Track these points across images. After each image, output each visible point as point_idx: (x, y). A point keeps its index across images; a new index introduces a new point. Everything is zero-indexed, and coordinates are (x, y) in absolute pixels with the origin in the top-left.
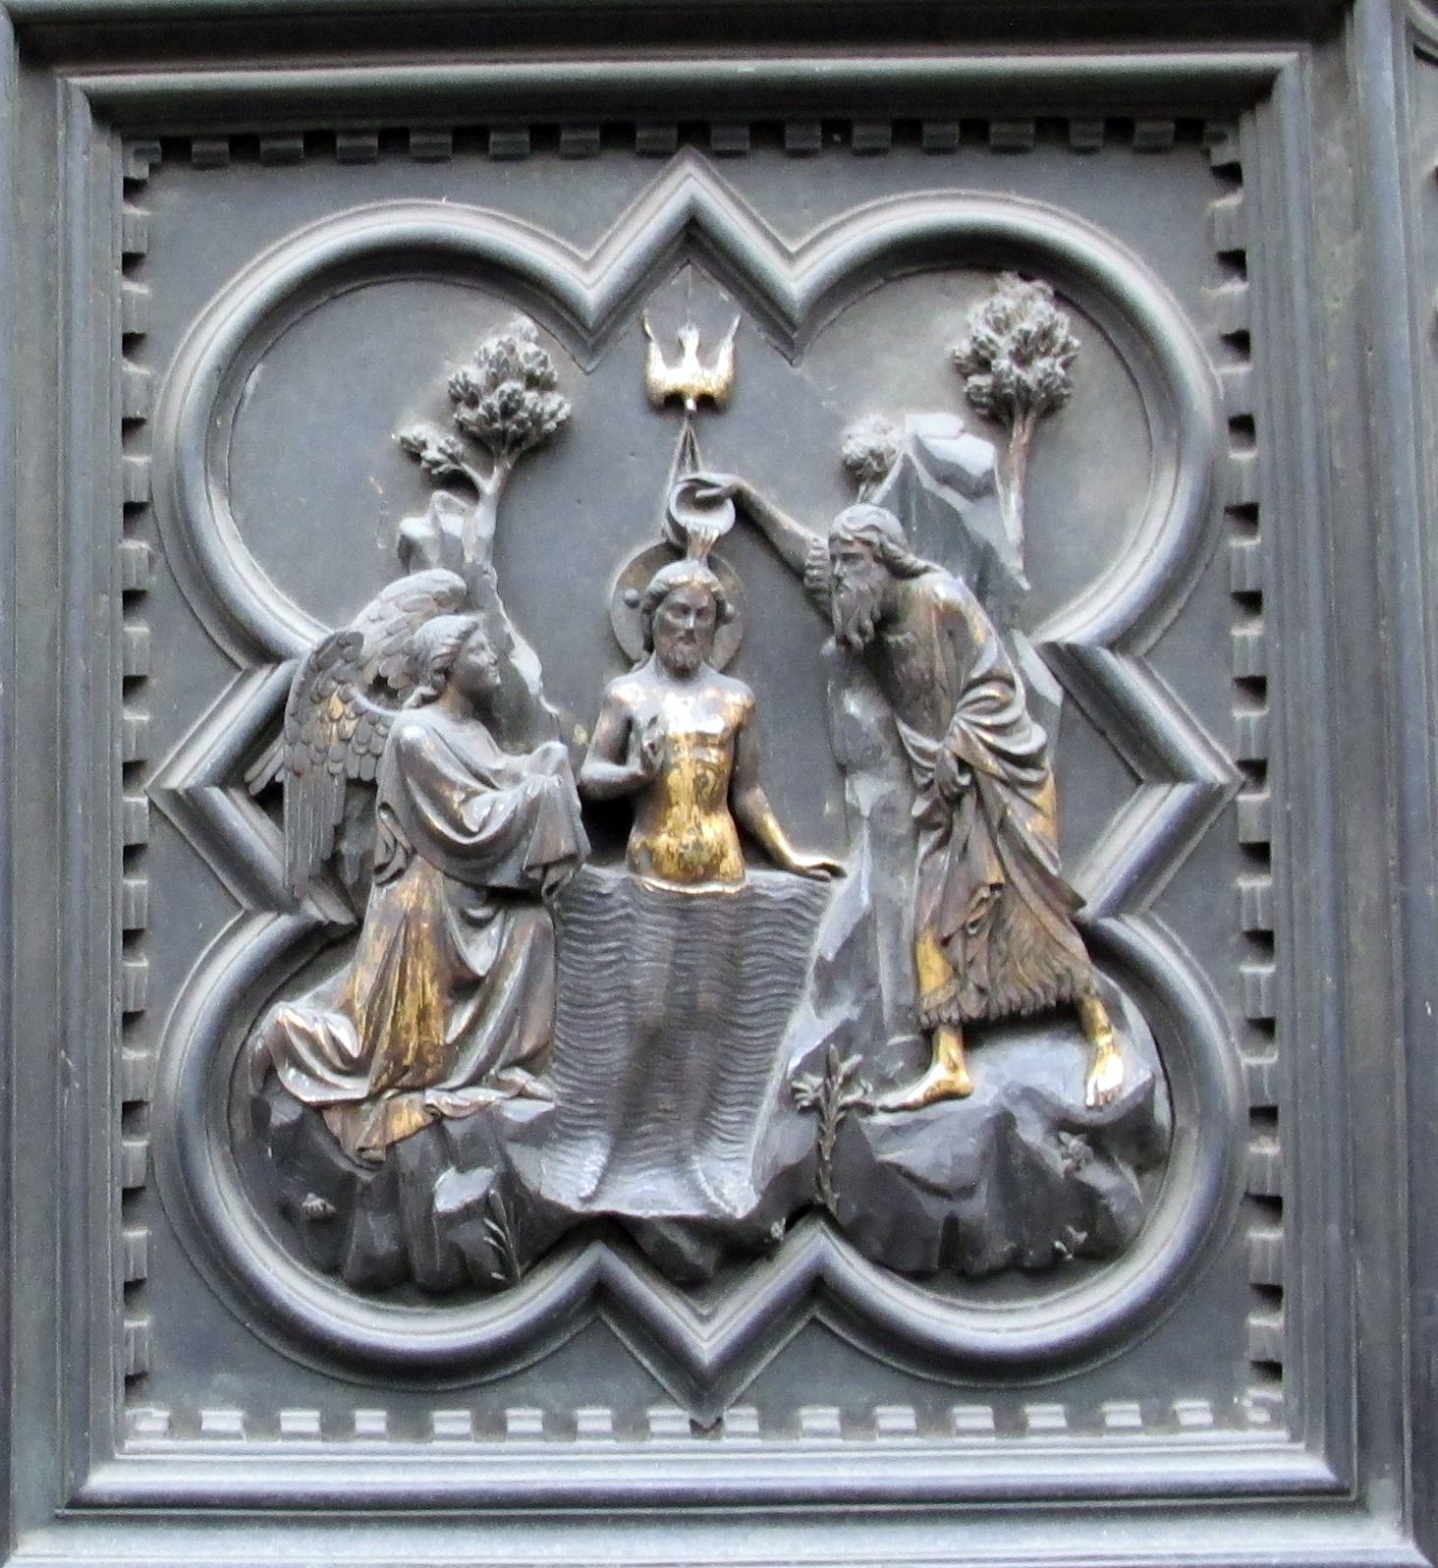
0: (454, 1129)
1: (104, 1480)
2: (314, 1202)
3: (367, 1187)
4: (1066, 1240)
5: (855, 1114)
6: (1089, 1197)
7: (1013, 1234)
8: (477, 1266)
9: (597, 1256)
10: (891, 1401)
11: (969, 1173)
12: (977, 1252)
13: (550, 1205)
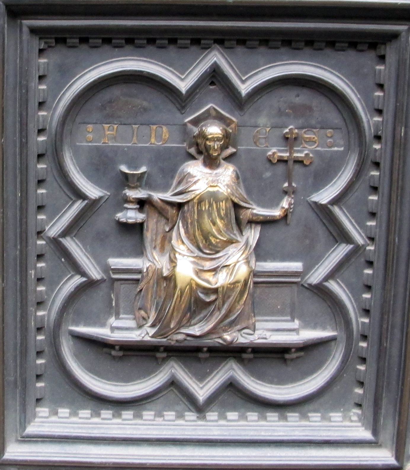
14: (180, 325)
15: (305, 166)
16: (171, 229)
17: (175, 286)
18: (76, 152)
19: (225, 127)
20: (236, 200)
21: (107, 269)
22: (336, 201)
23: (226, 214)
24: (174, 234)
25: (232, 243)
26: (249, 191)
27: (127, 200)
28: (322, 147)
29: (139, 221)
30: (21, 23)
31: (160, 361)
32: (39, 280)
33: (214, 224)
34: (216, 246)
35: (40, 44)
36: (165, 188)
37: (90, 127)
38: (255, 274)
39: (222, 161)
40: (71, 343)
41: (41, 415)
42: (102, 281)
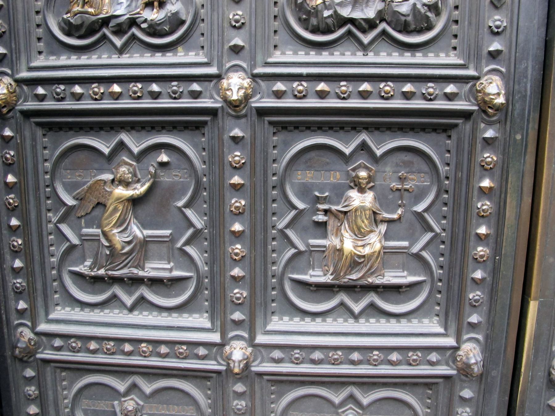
0: (327, 3)
1: (270, 60)
2: (304, 16)
3: (313, 12)
4: (423, 25)
5: (391, 3)
6: (428, 17)
7: (415, 25)
8: (330, 26)
9: (349, 26)
10: (395, 52)
11: (409, 12)
12: (409, 26)
13: (342, 16)
14: (345, 274)
15: (410, 192)
16: (341, 225)
17: (343, 254)
18: (292, 185)
19: (369, 172)
20: (374, 210)
21: (308, 245)
22: (426, 210)
23: (369, 217)
24: (343, 227)
25: (372, 232)
26: (381, 205)
27: (318, 210)
28: (419, 183)
29: (325, 220)
30: (264, 119)
31: (335, 292)
32: (273, 251)
33: (363, 222)
34: (364, 234)
35: (273, 130)
36: (338, 204)
37: (299, 172)
38: (384, 248)
39: (367, 190)
40: (290, 283)
41: (274, 320)
42: (306, 251)
